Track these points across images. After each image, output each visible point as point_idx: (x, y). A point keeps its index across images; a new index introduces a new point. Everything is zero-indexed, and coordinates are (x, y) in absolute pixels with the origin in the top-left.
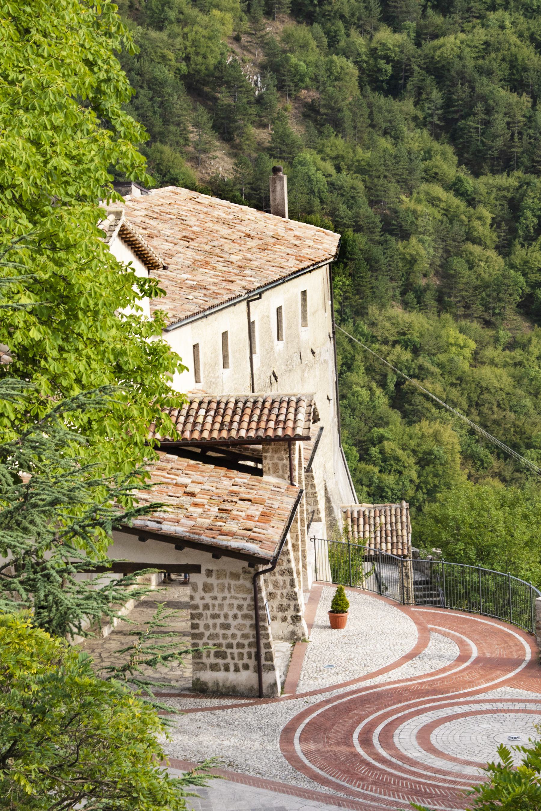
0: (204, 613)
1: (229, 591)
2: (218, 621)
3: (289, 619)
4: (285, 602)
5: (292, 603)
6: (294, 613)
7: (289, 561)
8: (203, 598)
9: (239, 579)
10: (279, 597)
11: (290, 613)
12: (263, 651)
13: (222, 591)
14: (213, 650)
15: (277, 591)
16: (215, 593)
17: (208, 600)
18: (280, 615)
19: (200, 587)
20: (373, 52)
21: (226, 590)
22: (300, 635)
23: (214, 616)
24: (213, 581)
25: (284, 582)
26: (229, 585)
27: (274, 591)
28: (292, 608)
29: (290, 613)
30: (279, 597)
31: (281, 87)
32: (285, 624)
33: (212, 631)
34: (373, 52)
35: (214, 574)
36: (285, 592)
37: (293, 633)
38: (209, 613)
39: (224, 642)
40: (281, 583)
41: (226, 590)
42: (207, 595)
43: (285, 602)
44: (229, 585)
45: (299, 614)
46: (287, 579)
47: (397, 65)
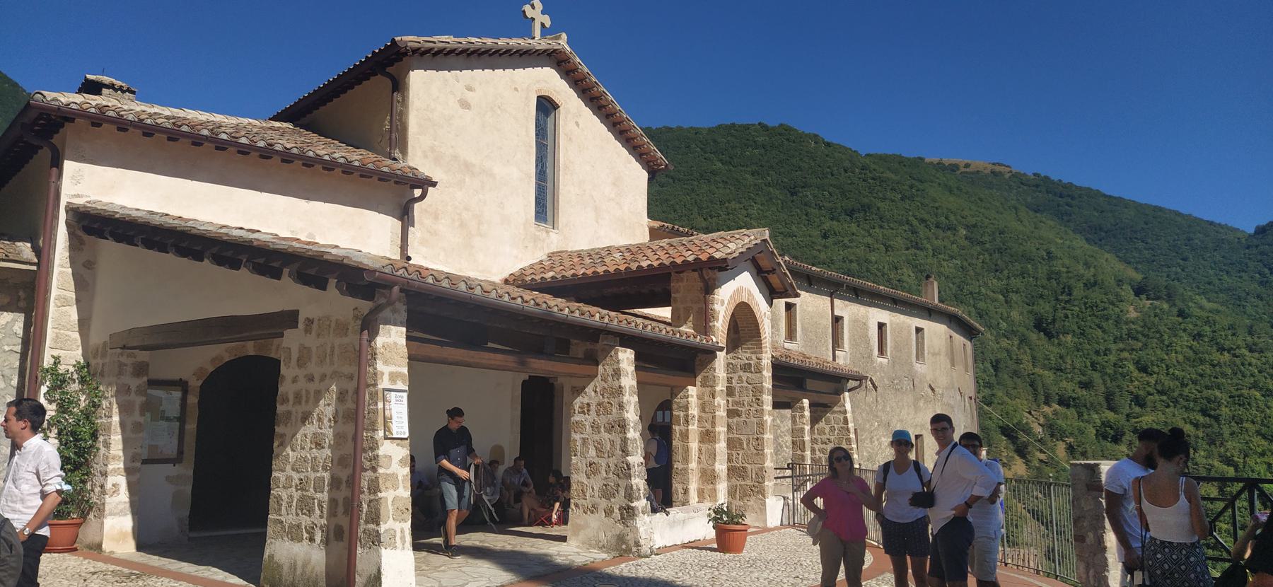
0: (294, 410)
1: (332, 363)
3: (616, 511)
5: (623, 483)
6: (624, 502)
7: (621, 406)
8: (295, 380)
9: (346, 335)
11: (619, 500)
13: (321, 362)
16: (313, 368)
17: (302, 384)
18: (603, 503)
19: (295, 356)
20: (1103, 423)
21: (328, 360)
22: (632, 543)
24: (311, 341)
25: (612, 442)
26: (333, 348)
27: (596, 460)
31: (1052, 435)
32: (610, 521)
34: (1103, 423)
35: (315, 326)
36: (612, 461)
37: (621, 539)
41: (328, 360)
42: (301, 373)
44: (333, 348)
47: (1116, 431)
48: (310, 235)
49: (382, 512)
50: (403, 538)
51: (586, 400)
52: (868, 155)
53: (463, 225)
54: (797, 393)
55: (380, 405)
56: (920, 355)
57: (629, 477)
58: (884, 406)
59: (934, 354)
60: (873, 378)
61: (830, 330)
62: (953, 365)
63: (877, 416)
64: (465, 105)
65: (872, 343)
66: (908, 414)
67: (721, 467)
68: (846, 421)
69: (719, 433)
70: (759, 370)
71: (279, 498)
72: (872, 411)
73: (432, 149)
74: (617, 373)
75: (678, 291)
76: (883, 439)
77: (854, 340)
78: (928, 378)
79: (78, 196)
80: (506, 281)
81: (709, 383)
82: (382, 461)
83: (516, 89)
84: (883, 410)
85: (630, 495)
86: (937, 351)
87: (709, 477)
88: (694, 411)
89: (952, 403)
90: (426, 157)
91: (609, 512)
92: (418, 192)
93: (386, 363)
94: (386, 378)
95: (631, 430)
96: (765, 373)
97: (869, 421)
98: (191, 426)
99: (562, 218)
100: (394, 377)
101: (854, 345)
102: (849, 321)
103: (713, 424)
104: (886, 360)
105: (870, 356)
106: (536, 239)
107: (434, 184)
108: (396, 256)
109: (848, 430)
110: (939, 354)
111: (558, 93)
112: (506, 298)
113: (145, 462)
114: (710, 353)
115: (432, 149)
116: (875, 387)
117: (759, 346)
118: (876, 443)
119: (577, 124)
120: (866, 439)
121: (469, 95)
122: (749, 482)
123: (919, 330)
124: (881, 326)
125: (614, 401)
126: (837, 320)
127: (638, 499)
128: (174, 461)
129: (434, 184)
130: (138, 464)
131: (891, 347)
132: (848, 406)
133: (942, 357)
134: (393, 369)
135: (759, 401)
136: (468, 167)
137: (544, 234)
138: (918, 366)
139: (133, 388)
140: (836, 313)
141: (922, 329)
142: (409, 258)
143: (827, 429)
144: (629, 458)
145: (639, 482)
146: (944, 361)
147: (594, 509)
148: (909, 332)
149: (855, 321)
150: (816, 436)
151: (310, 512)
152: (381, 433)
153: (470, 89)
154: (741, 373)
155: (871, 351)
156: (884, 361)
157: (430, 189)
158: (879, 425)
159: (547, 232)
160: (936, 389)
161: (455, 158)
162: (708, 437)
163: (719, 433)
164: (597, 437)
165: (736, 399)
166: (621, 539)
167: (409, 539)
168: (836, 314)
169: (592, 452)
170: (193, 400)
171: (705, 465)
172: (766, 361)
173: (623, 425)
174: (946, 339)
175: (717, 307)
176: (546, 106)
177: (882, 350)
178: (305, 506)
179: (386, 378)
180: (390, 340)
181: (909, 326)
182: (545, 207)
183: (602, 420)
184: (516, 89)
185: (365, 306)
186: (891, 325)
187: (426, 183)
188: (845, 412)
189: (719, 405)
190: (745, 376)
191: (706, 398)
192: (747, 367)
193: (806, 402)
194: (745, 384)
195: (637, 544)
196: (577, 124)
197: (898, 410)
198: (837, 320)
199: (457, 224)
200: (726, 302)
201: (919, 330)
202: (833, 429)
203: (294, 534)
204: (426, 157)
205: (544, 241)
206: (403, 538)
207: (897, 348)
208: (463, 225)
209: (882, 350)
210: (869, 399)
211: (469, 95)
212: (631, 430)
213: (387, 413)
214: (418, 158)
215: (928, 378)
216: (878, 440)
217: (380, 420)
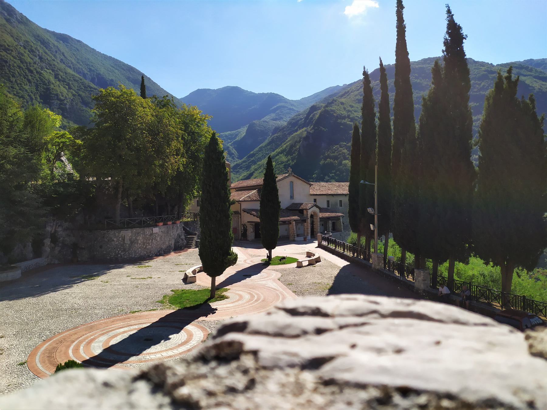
52: (498, 65)
80: (286, 208)
81: (308, 222)
85: (295, 235)
98: (254, 229)
99: (294, 197)
132: (341, 220)
166: (294, 240)
170: (254, 226)
172: (318, 218)
175: (308, 214)
176: (292, 183)
182: (292, 197)
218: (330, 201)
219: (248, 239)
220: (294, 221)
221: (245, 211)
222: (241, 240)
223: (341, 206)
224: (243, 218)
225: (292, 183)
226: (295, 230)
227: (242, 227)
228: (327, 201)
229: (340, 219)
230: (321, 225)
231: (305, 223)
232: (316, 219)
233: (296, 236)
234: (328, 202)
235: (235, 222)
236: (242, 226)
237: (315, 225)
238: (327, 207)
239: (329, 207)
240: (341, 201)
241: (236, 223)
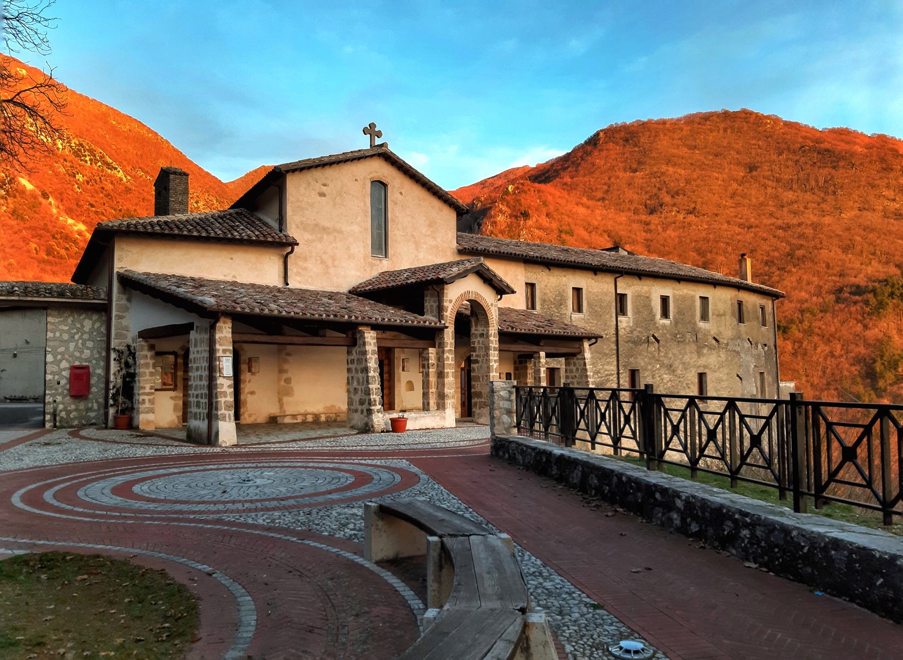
2: (199, 373)
3: (365, 411)
4: (364, 397)
5: (367, 398)
7: (366, 360)
10: (360, 392)
11: (365, 407)
12: (214, 401)
14: (196, 400)
15: (359, 387)
17: (196, 355)
18: (360, 408)
23: (197, 369)
24: (198, 336)
27: (357, 387)
28: (367, 401)
29: (365, 407)
30: (360, 392)
32: (362, 416)
33: (196, 383)
36: (363, 387)
37: (366, 424)
38: (195, 366)
39: (199, 392)
40: (361, 380)
42: (196, 350)
43: (364, 397)
45: (373, 408)
46: (364, 375)
48: (234, 277)
49: (219, 407)
50: (230, 417)
51: (352, 357)
53: (323, 262)
54: (534, 348)
55: (218, 363)
56: (704, 317)
57: (370, 394)
58: (666, 353)
59: (719, 315)
60: (655, 335)
61: (614, 304)
62: (741, 320)
63: (659, 360)
64: (322, 195)
65: (654, 310)
66: (691, 359)
67: (449, 391)
68: (585, 364)
69: (448, 373)
70: (488, 336)
71: (190, 402)
72: (654, 357)
73: (302, 223)
74: (364, 344)
75: (427, 296)
76: (665, 376)
77: (637, 309)
78: (712, 333)
79: (122, 268)
80: (350, 292)
81: (441, 346)
82: (219, 386)
83: (356, 180)
84: (665, 356)
86: (722, 312)
87: (441, 396)
88: (433, 360)
89: (738, 349)
90: (298, 227)
91: (362, 412)
92: (289, 249)
93: (220, 345)
94: (221, 351)
95: (372, 372)
96: (491, 338)
97: (650, 364)
99: (391, 251)
100: (224, 351)
101: (637, 311)
102: (632, 296)
103: (444, 368)
104: (669, 322)
105: (652, 319)
106: (372, 265)
107: (298, 244)
108: (280, 285)
109: (586, 370)
110: (724, 315)
111: (386, 177)
112: (284, 313)
113: (156, 390)
114: (441, 330)
115: (302, 223)
116: (658, 341)
117: (487, 324)
118: (658, 379)
119: (401, 193)
120: (648, 376)
121: (324, 189)
122: (483, 400)
123: (704, 299)
124: (665, 300)
125: (363, 358)
126: (621, 299)
127: (375, 405)
128: (174, 390)
129: (298, 244)
130: (153, 391)
131: (674, 312)
132: (588, 355)
133: (728, 317)
134: (224, 347)
135: (488, 355)
136: (325, 229)
137: (378, 262)
138: (702, 325)
139: (149, 356)
140: (618, 292)
141: (707, 298)
142: (287, 284)
143: (574, 369)
144: (370, 386)
145: (376, 397)
146: (731, 320)
147: (356, 411)
148: (693, 301)
149: (638, 296)
150: (568, 374)
151: (199, 408)
152: (218, 375)
153: (325, 185)
154: (479, 339)
155: (654, 316)
156: (666, 322)
157: (296, 247)
158: (661, 367)
159: (380, 260)
160: (721, 340)
161: (316, 225)
162: (441, 375)
163: (448, 373)
164: (357, 375)
165: (477, 353)
166: (366, 424)
167: (233, 418)
168: (618, 292)
169: (355, 383)
171: (439, 390)
172: (493, 330)
173: (366, 370)
174: (732, 304)
175: (445, 304)
176: (380, 185)
177: (665, 314)
178: (198, 405)
179: (221, 351)
180: (223, 335)
181: (693, 297)
183: (359, 367)
184: (356, 180)
185: (212, 321)
186: (674, 296)
187: (293, 244)
188: (585, 359)
189: (448, 358)
190: (481, 340)
191: (440, 354)
192: (482, 335)
193: (542, 354)
194: (481, 345)
195: (373, 426)
196: (401, 193)
197: (681, 356)
198: (621, 299)
199: (319, 262)
200: (454, 302)
201: (704, 299)
202: (577, 369)
203: (196, 416)
204: (298, 227)
205: (378, 265)
206: (230, 417)
207: (680, 312)
208: (323, 262)
209: (665, 314)
210: (652, 349)
211: (324, 189)
212: (372, 372)
213: (221, 366)
214: (293, 231)
215: (712, 333)
216: (659, 376)
217: (218, 369)
218: (537, 287)
219: (135, 423)
220: (375, 327)
221: (130, 284)
222: (106, 428)
223: (579, 309)
224: (119, 317)
225: (380, 185)
226: (371, 374)
227: (113, 363)
228: (527, 284)
229: (581, 351)
230: (504, 376)
231: (431, 350)
232: (482, 335)
233: (379, 407)
234: (531, 286)
235: (86, 336)
236: (113, 355)
237: (477, 362)
238: (528, 309)
239: (533, 307)
240: (578, 291)
241: (90, 344)
